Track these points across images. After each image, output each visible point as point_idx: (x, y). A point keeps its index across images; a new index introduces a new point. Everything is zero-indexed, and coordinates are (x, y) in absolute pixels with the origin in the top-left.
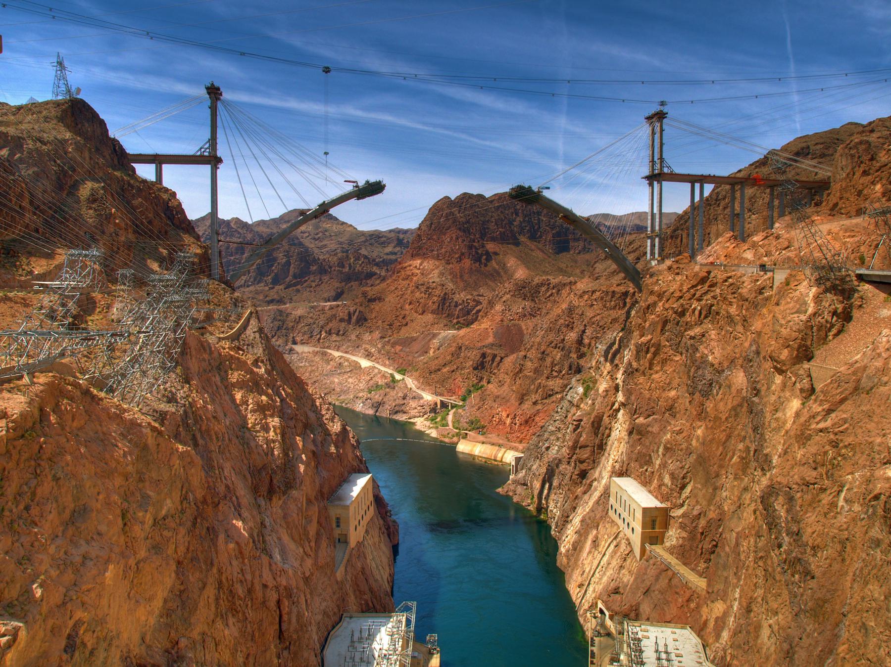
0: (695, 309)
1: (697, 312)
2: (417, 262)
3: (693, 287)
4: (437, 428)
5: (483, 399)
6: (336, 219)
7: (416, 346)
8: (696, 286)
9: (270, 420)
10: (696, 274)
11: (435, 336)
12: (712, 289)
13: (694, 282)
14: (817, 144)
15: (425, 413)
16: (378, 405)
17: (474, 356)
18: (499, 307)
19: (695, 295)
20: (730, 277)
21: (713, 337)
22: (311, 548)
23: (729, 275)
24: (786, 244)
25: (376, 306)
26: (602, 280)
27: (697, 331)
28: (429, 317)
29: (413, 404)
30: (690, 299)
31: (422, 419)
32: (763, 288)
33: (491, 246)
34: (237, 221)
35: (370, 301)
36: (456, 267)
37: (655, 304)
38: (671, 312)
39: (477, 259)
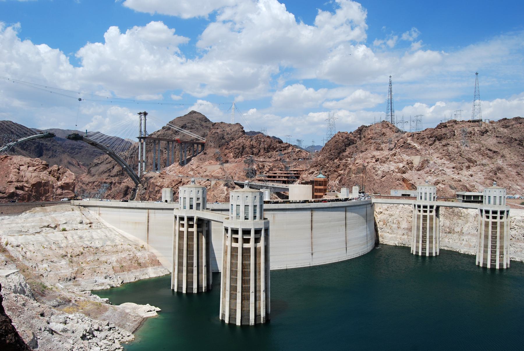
26: (96, 176)
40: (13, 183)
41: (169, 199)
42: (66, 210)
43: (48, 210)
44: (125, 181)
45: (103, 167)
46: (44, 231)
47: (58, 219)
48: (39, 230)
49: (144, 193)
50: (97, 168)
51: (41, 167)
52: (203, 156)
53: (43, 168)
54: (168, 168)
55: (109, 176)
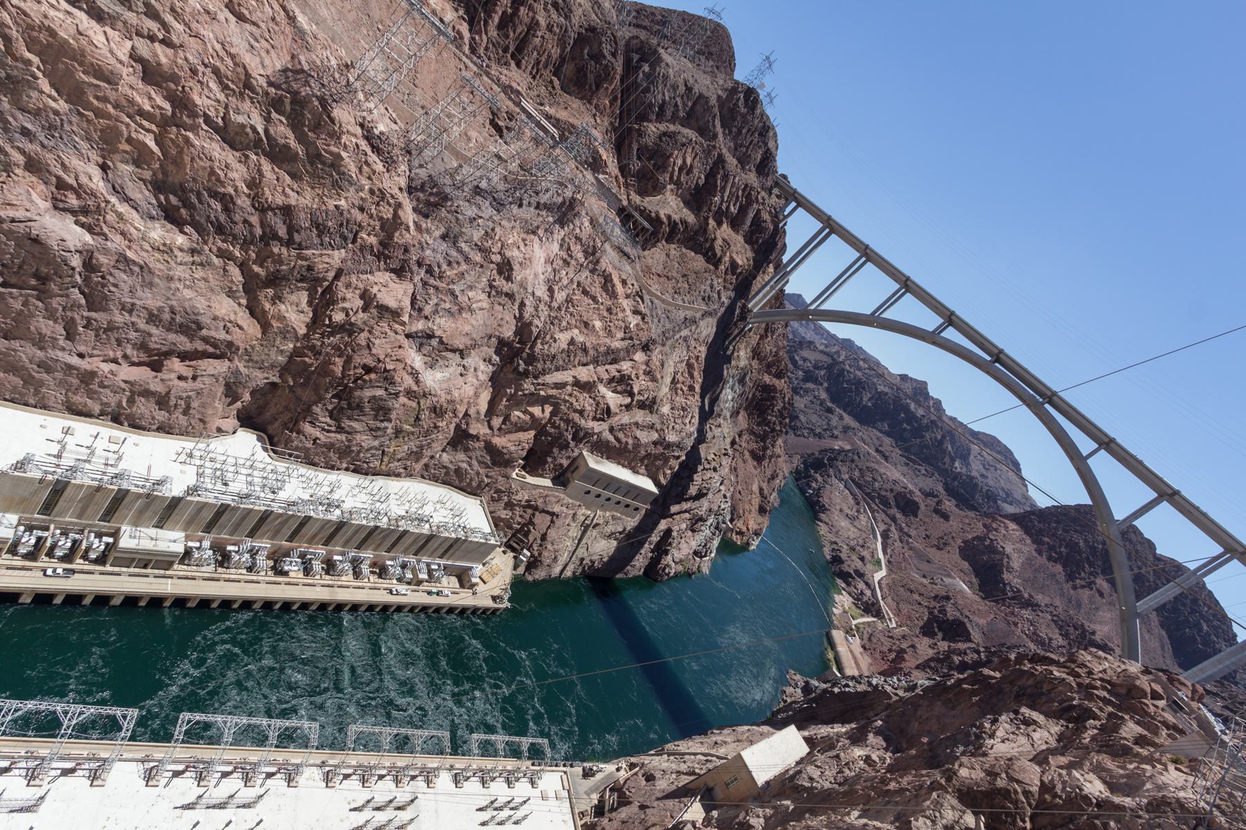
2: (1012, 526)
4: (845, 612)
5: (904, 637)
6: (1020, 470)
7: (925, 567)
9: (576, 331)
11: (949, 576)
15: (858, 599)
16: (837, 560)
17: (951, 613)
18: (1026, 613)
21: (1036, 736)
22: (500, 429)
25: (936, 518)
27: (1036, 716)
28: (966, 565)
29: (861, 586)
31: (851, 599)
33: (1101, 583)
34: (938, 403)
35: (936, 511)
36: (1042, 560)
39: (1071, 577)
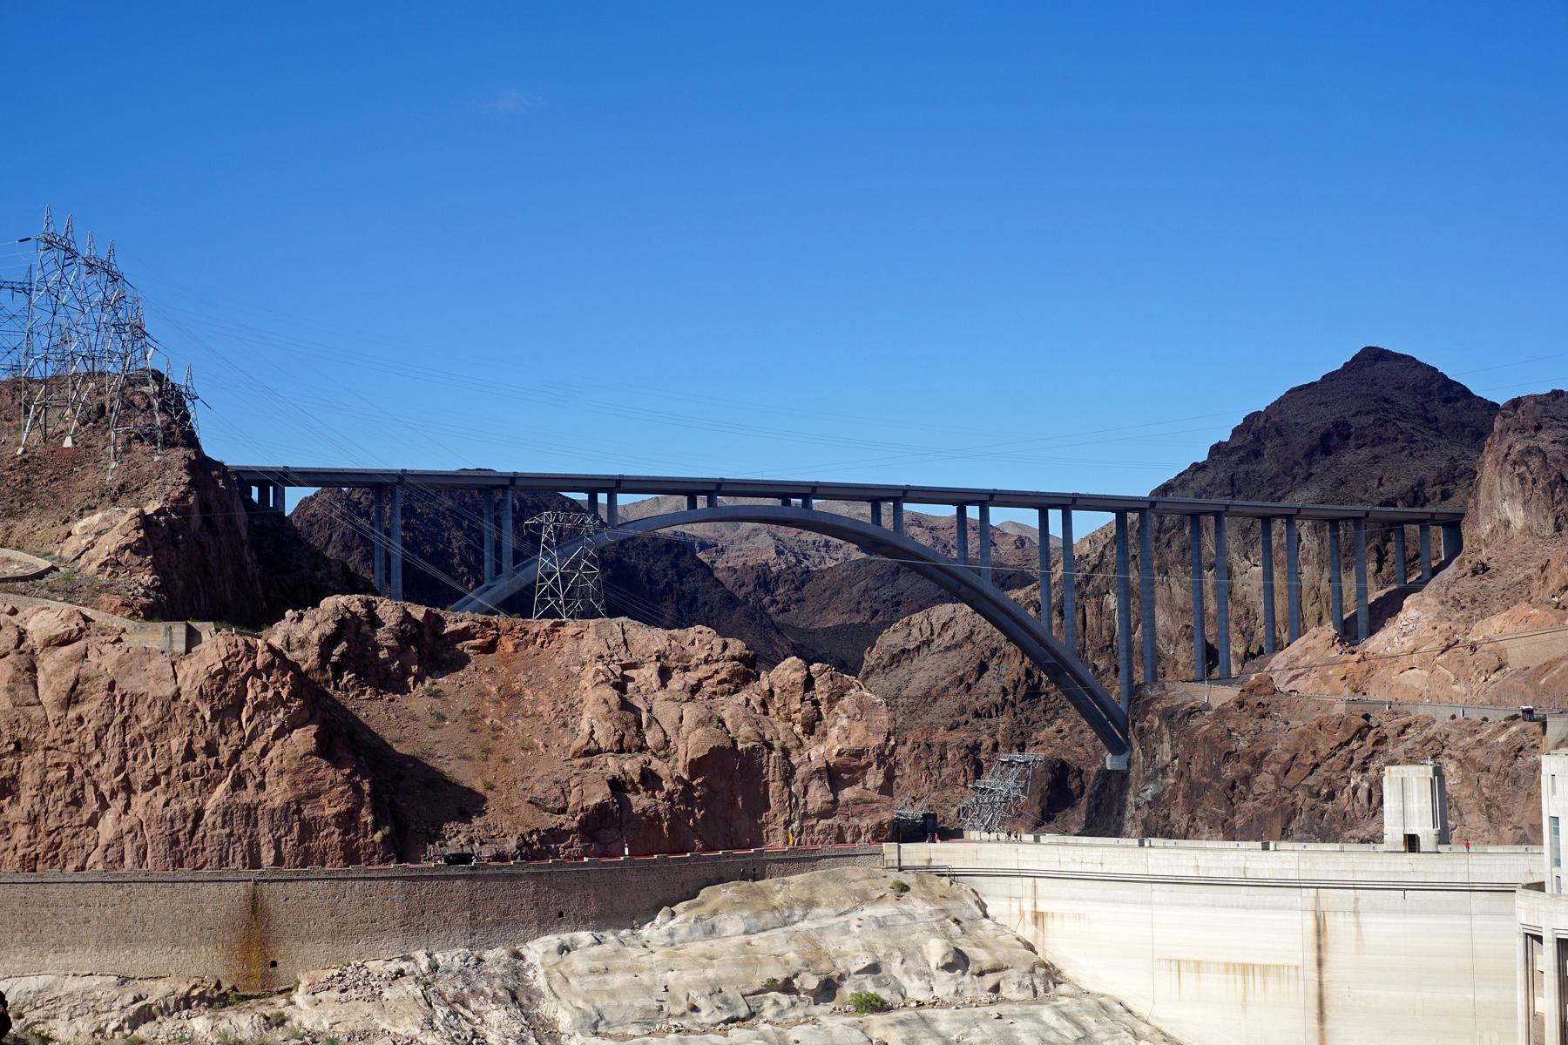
0: (1355, 790)
1: (1362, 794)
3: (1341, 746)
8: (1348, 743)
10: (1342, 722)
12: (1381, 748)
13: (1340, 736)
14: (1357, 413)
19: (1351, 760)
20: (1409, 726)
23: (1405, 720)
24: (1496, 665)
30: (1344, 769)
32: (1521, 749)
37: (1247, 779)
38: (1301, 794)
40: (599, 760)
41: (1425, 830)
42: (865, 898)
43: (778, 899)
44: (1041, 736)
45: (926, 671)
46: (769, 1012)
47: (831, 943)
48: (743, 1011)
49: (1156, 797)
50: (901, 672)
51: (726, 668)
52: (1470, 584)
53: (734, 674)
54: (1279, 660)
55: (962, 710)
